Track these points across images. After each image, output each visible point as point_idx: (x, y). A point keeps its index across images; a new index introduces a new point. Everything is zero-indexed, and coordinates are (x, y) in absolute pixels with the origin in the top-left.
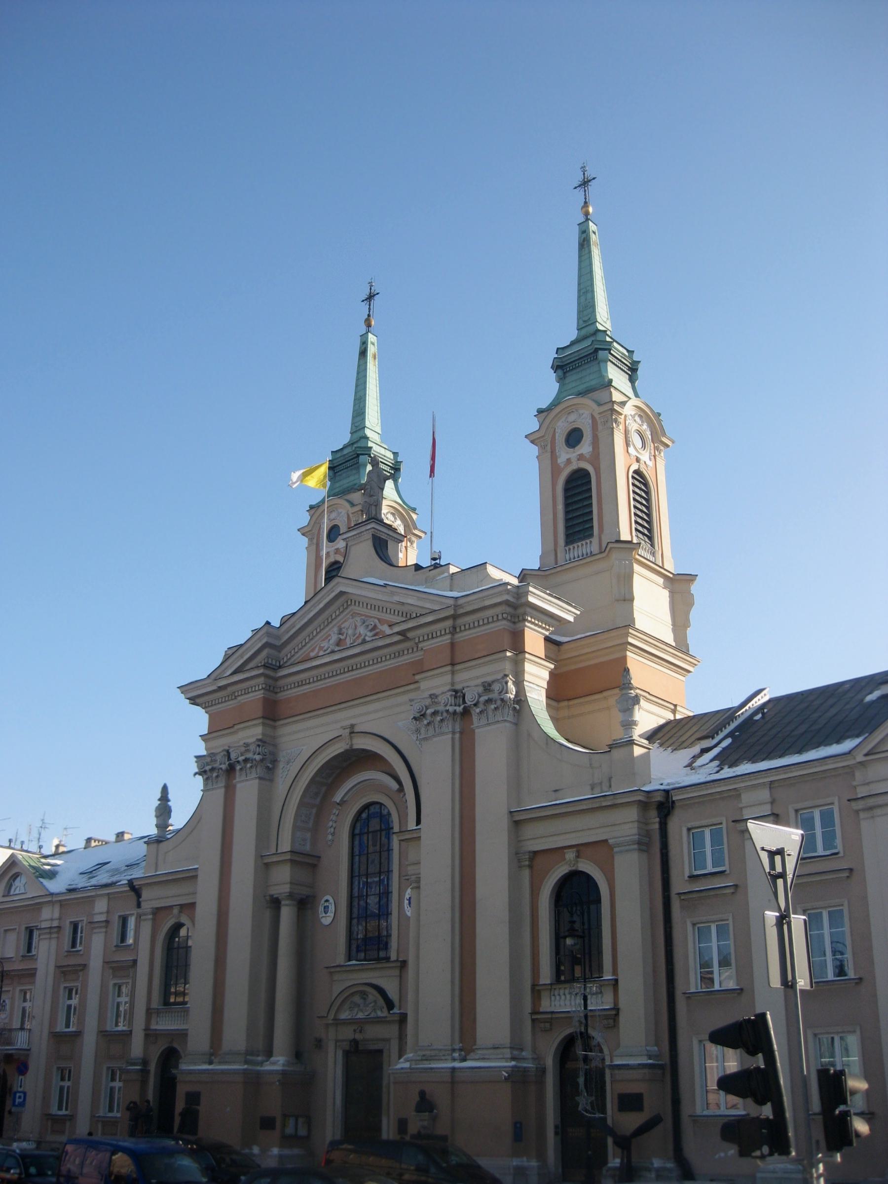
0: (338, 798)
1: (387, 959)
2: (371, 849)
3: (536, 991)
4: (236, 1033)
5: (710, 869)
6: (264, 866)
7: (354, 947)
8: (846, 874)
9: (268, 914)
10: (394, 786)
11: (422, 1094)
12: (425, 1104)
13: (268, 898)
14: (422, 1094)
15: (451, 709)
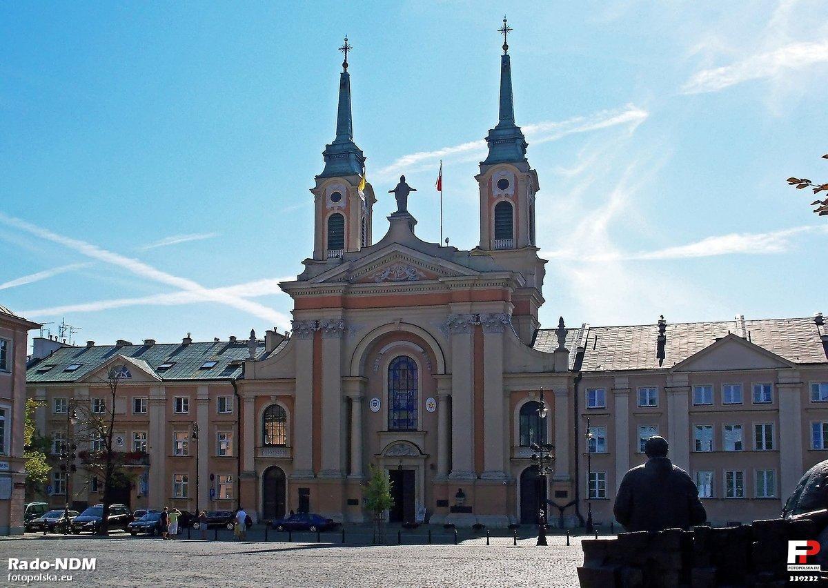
0: (382, 351)
1: (416, 430)
2: (401, 377)
3: (512, 448)
4: (332, 459)
5: (596, 406)
6: (345, 379)
7: (392, 422)
8: (660, 414)
9: (345, 405)
10: (422, 350)
11: (460, 490)
12: (460, 494)
13: (345, 397)
14: (460, 490)
15: (473, 323)
